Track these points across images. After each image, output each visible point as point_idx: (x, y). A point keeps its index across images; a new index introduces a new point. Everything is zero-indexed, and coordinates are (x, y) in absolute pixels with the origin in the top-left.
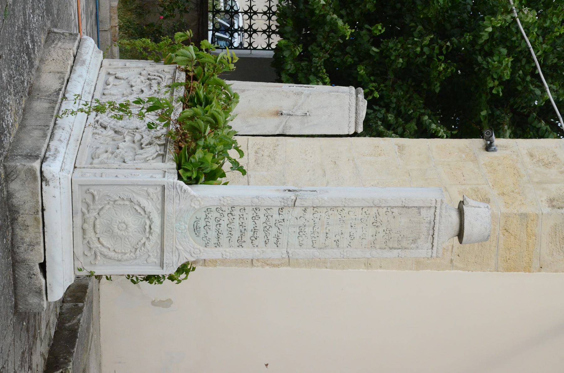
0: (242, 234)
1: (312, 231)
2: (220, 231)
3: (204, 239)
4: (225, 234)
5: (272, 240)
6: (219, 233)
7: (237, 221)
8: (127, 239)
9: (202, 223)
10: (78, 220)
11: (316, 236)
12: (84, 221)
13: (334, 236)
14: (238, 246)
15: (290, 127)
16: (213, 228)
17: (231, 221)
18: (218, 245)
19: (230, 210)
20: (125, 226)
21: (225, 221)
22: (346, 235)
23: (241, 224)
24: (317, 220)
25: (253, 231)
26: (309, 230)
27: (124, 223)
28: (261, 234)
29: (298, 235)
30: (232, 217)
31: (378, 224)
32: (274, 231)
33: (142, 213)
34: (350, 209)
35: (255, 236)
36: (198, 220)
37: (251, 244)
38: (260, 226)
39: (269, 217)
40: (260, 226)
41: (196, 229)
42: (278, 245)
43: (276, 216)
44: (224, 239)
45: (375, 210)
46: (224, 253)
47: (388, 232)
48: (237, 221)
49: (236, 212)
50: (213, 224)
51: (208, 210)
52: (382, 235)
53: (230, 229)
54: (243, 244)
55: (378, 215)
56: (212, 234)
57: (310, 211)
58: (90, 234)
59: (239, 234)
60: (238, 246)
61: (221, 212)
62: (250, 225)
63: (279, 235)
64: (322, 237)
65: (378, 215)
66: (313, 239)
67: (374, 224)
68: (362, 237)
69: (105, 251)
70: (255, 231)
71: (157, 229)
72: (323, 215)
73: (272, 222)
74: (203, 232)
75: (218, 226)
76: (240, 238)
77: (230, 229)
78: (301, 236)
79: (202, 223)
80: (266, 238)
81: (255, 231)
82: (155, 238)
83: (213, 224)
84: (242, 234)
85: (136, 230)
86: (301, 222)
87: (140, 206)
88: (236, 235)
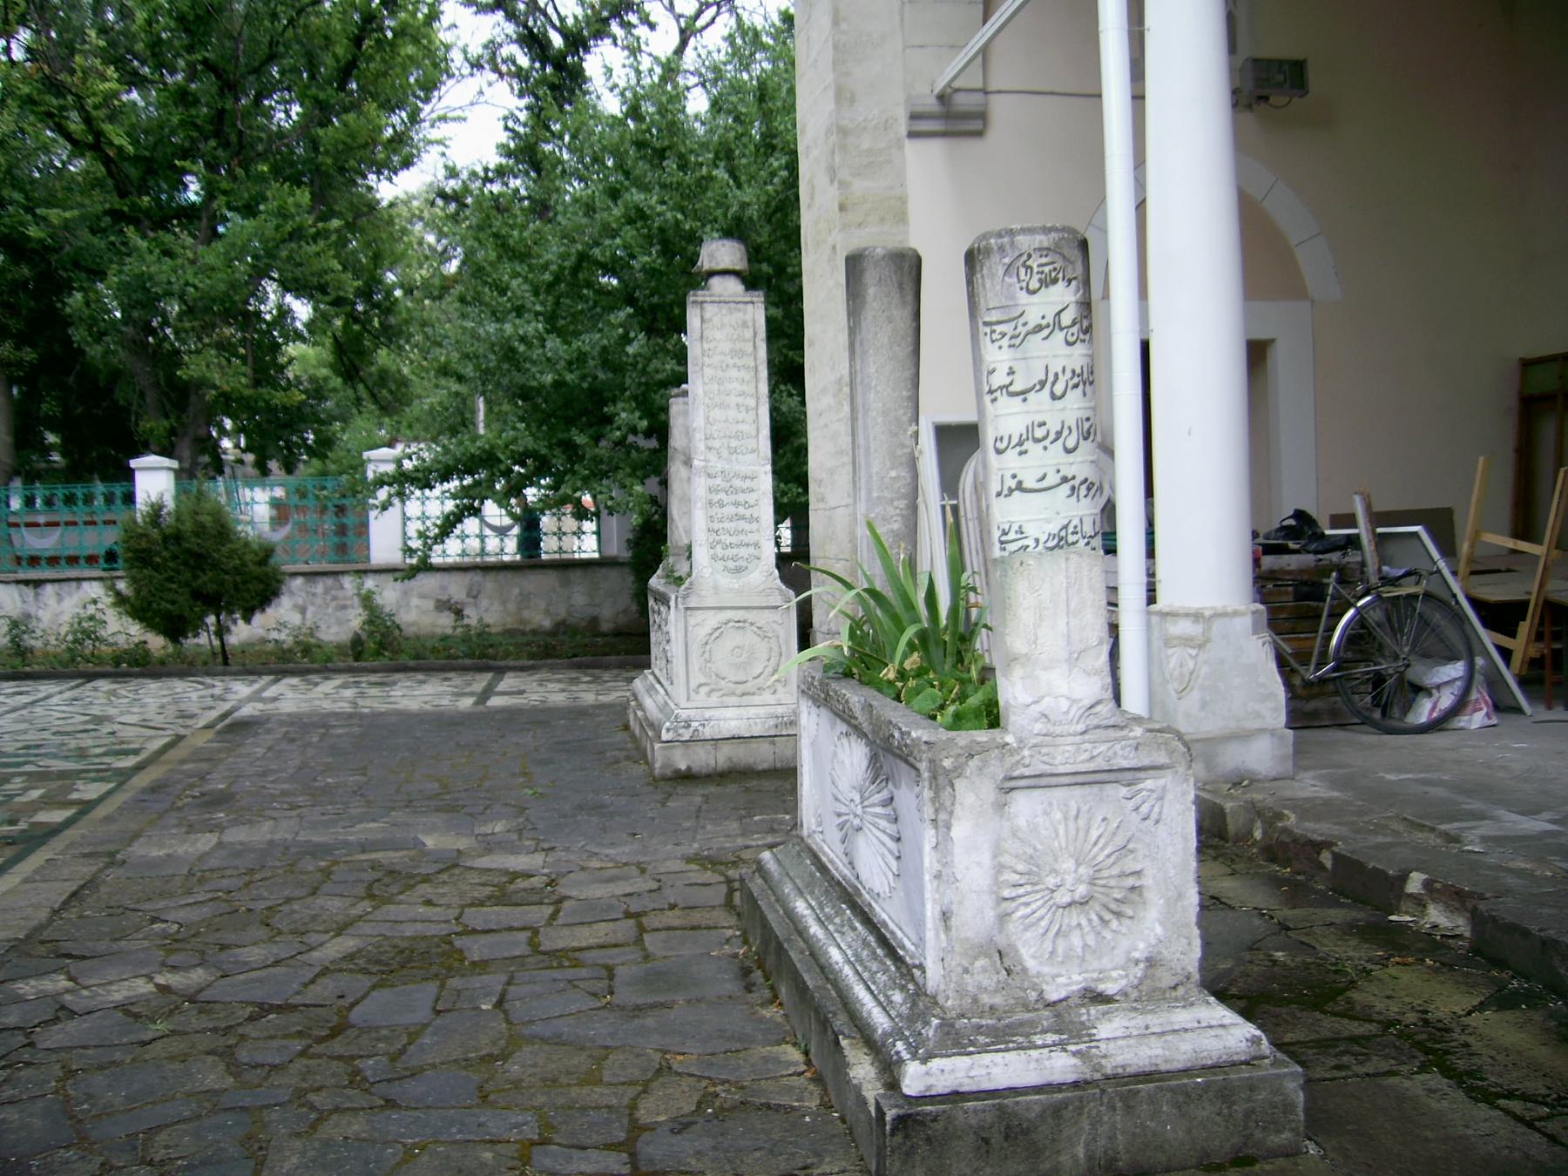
0: (743, 518)
4: (742, 537)
5: (748, 483)
6: (741, 545)
7: (726, 525)
9: (731, 564)
10: (733, 700)
12: (733, 694)
16: (735, 551)
18: (757, 545)
21: (728, 539)
22: (740, 400)
26: (734, 443)
28: (741, 497)
32: (737, 483)
36: (726, 568)
38: (732, 498)
40: (732, 498)
41: (738, 570)
43: (718, 481)
44: (750, 538)
45: (706, 370)
48: (726, 525)
49: (716, 526)
50: (730, 552)
51: (714, 558)
56: (744, 552)
57: (711, 443)
58: (748, 687)
62: (731, 510)
64: (741, 427)
69: (770, 669)
70: (736, 504)
71: (739, 615)
74: (743, 563)
79: (731, 564)
81: (736, 504)
82: (751, 616)
83: (730, 552)
84: (743, 518)
86: (725, 453)
88: (742, 525)
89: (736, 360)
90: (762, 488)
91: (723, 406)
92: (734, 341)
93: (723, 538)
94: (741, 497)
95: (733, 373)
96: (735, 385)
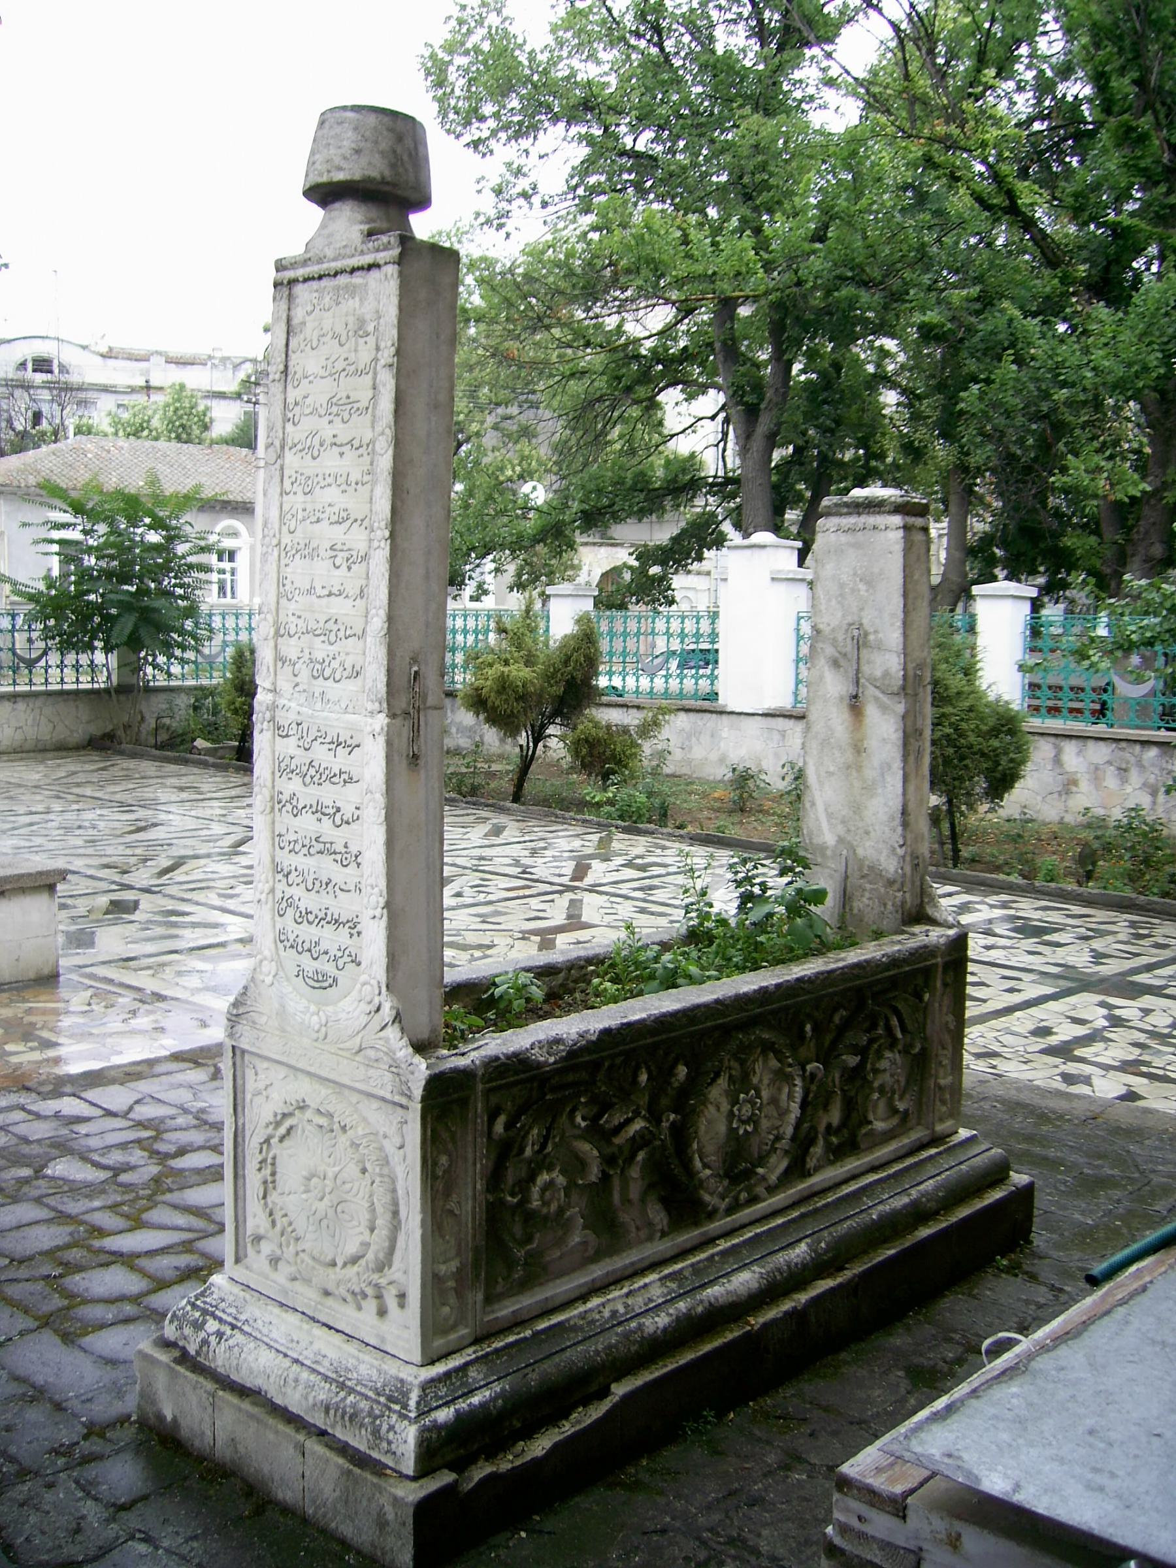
0: (327, 850)
1: (322, 638)
2: (321, 915)
3: (341, 963)
4: (327, 900)
8: (348, 1186)
11: (335, 628)
13: (337, 572)
14: (359, 865)
15: (886, 674)
17: (300, 879)
18: (353, 926)
19: (280, 876)
20: (315, 1180)
22: (337, 533)
23: (305, 851)
24: (302, 625)
25: (319, 815)
26: (321, 650)
27: (309, 1179)
28: (328, 794)
29: (330, 682)
30: (294, 874)
31: (316, 441)
32: (321, 754)
33: (288, 1123)
34: (285, 529)
35: (332, 811)
37: (353, 826)
39: (293, 767)
42: (354, 742)
46: (371, 913)
47: (335, 409)
50: (308, 932)
52: (342, 426)
53: (318, 884)
54: (354, 849)
55: (299, 447)
59: (327, 861)
60: (359, 865)
61: (284, 905)
62: (307, 824)
63: (328, 740)
65: (299, 447)
66: (341, 634)
67: (316, 453)
68: (344, 487)
70: (319, 810)
72: (292, 607)
73: (301, 758)
75: (311, 918)
76: (338, 857)
77: (318, 884)
78: (334, 671)
80: (335, 780)
81: (319, 810)
83: (308, 932)
84: (327, 850)
85: (326, 1154)
86: (304, 674)
87: (278, 1124)
88: (327, 867)
89: (338, 426)
90: (367, 776)
91: (309, 552)
92: (335, 376)
93: (297, 892)
94: (328, 794)
95: (331, 462)
96: (331, 495)
